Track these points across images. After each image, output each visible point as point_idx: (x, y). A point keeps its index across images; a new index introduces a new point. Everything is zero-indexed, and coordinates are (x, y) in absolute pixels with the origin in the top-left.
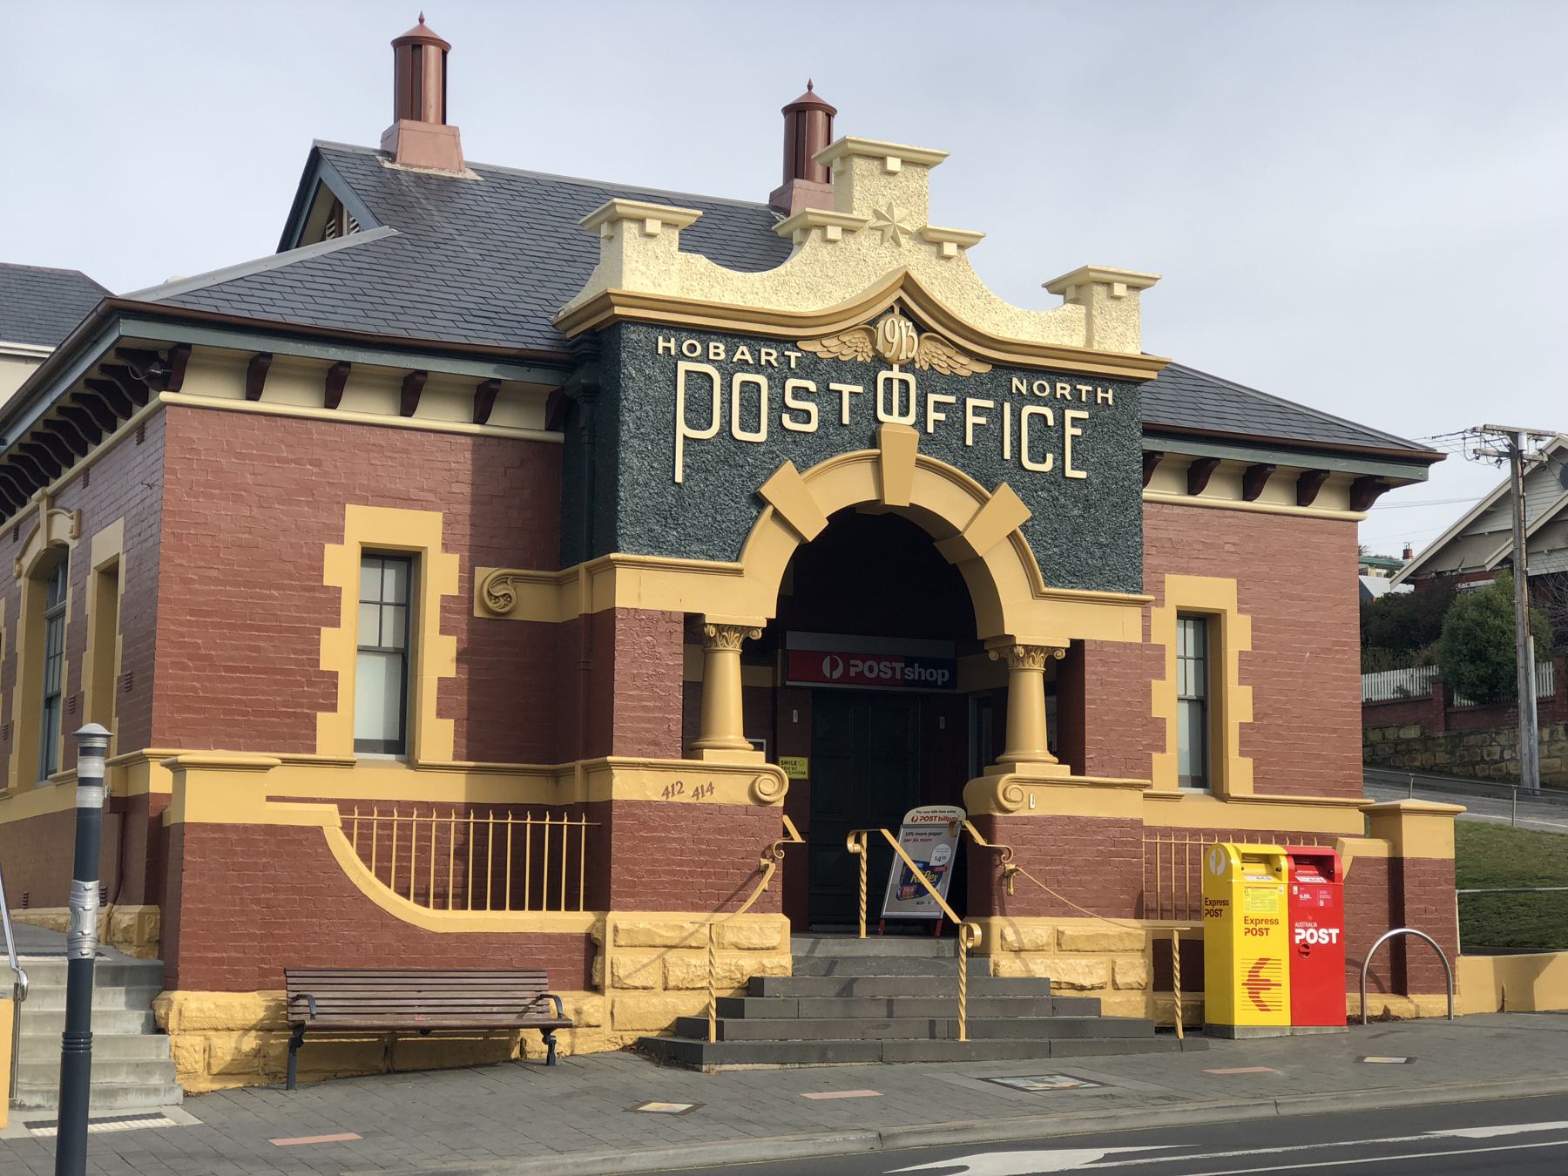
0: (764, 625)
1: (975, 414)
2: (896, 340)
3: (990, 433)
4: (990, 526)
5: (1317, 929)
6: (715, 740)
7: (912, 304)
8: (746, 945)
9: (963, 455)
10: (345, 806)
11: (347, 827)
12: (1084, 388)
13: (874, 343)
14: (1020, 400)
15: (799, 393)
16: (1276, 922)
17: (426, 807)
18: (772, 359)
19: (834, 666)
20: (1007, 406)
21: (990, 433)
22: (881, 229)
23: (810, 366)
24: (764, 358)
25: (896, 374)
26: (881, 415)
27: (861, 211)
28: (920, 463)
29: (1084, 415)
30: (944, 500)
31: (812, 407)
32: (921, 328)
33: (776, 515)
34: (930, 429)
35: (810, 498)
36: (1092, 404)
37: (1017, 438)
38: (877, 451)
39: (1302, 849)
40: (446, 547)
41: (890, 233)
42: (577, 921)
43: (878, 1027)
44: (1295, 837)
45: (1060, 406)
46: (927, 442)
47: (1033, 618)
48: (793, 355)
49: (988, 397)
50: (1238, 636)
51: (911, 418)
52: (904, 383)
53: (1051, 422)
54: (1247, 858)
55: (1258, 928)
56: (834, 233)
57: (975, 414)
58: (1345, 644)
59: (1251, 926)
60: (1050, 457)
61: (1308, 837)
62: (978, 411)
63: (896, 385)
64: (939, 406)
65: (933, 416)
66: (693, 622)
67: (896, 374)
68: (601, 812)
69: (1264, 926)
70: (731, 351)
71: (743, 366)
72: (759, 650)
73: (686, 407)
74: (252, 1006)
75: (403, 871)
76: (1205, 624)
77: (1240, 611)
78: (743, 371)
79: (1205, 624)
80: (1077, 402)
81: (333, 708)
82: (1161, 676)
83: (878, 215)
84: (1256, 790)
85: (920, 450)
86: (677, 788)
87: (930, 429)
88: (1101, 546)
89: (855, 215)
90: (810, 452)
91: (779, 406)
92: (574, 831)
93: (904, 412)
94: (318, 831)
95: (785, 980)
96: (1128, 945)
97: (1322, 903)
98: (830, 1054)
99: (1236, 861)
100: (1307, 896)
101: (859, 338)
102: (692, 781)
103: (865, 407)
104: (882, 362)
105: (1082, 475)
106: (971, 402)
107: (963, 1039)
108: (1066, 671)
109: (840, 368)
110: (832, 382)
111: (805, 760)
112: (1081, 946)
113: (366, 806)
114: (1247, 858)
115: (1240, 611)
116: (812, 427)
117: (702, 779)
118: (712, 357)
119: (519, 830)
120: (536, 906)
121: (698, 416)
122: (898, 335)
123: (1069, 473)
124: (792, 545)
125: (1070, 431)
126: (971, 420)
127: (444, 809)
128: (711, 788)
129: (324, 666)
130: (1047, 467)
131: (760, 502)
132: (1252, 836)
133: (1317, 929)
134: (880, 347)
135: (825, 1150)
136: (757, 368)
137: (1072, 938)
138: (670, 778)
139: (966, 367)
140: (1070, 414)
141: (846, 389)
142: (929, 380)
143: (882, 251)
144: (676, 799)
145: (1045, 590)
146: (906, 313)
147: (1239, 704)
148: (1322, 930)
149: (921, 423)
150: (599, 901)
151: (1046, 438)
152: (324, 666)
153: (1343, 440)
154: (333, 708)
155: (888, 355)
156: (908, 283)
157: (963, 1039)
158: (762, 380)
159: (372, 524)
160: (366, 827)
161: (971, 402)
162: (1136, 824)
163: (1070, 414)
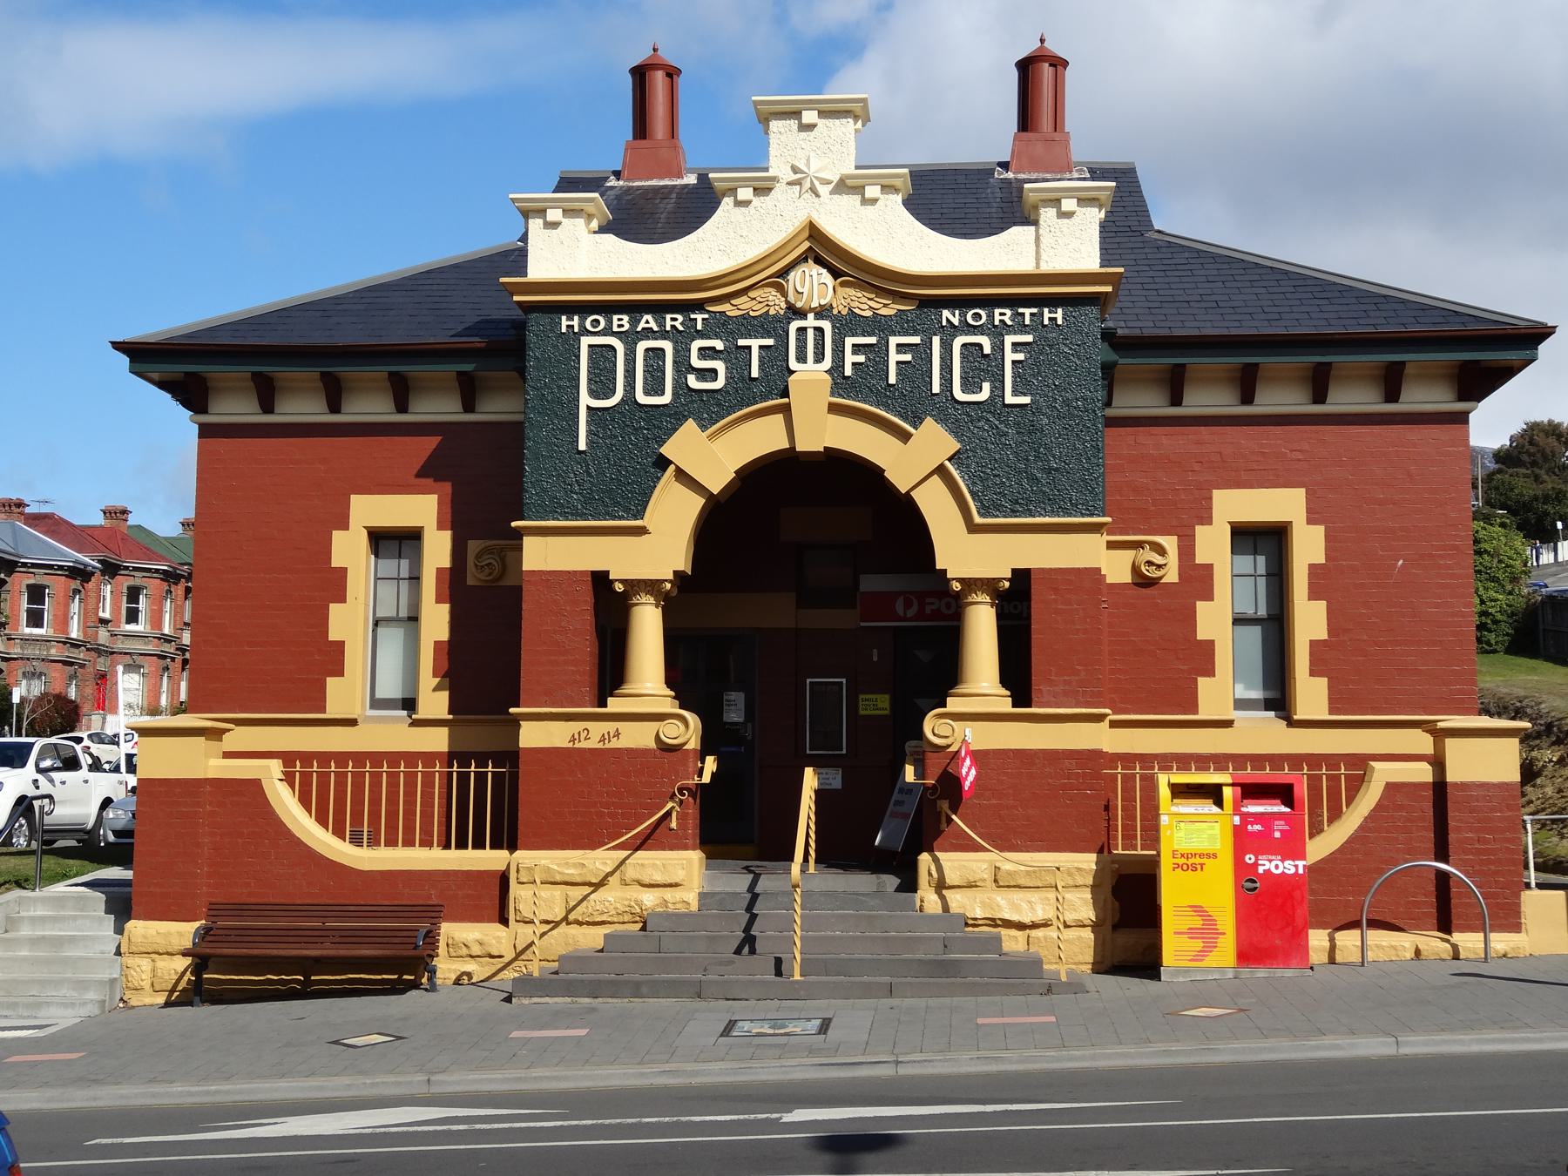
0: (671, 577)
1: (898, 352)
2: (806, 291)
3: (916, 370)
4: (913, 459)
5: (1282, 861)
6: (627, 689)
7: (819, 248)
8: (647, 881)
9: (885, 395)
10: (288, 758)
11: (288, 778)
12: (1027, 311)
13: (784, 294)
14: (953, 330)
15: (705, 353)
16: (1215, 856)
17: (411, 758)
18: (677, 324)
19: (908, 605)
20: (936, 340)
21: (916, 370)
22: (798, 183)
23: (719, 326)
24: (669, 324)
25: (811, 321)
26: (793, 364)
27: (778, 167)
28: (834, 409)
29: (1029, 338)
30: (757, 438)
31: (719, 366)
32: (836, 273)
33: (681, 475)
34: (848, 372)
35: (713, 456)
36: (1037, 325)
37: (946, 370)
38: (785, 400)
39: (1250, 774)
40: (440, 527)
41: (807, 185)
42: (490, 859)
43: (721, 964)
44: (1239, 760)
45: (997, 332)
46: (840, 383)
47: (964, 551)
48: (699, 317)
49: (915, 333)
50: (1308, 547)
51: (827, 363)
52: (819, 330)
53: (987, 350)
54: (1180, 791)
55: (1192, 863)
56: (745, 193)
57: (898, 352)
58: (1456, 548)
59: (1182, 861)
60: (986, 386)
61: (1258, 760)
62: (901, 348)
63: (810, 334)
64: (857, 349)
65: (850, 358)
66: (600, 580)
67: (811, 321)
68: (510, 756)
69: (1198, 860)
70: (634, 322)
71: (648, 333)
72: (679, 599)
73: (590, 380)
74: (183, 932)
75: (340, 812)
76: (1263, 541)
77: (1310, 521)
78: (648, 338)
79: (1263, 541)
80: (1022, 328)
81: (341, 673)
82: (1209, 596)
83: (795, 170)
84: (1331, 713)
85: (832, 395)
86: (583, 735)
87: (848, 372)
88: (1049, 471)
89: (771, 173)
90: (709, 410)
91: (682, 366)
92: (481, 778)
93: (819, 357)
94: (256, 783)
95: (689, 915)
96: (1080, 881)
97: (1277, 835)
98: (644, 990)
99: (1164, 792)
100: (1258, 827)
101: (772, 295)
102: (598, 729)
103: (776, 360)
104: (796, 312)
105: (1026, 400)
106: (894, 341)
107: (797, 977)
108: (1016, 597)
109: (752, 326)
110: (736, 336)
111: (887, 697)
112: (1022, 882)
113: (306, 757)
114: (1180, 791)
115: (1310, 521)
116: (719, 383)
117: (610, 726)
118: (615, 329)
119: (393, 777)
120: (409, 843)
121: (601, 386)
122: (813, 285)
123: (1010, 399)
124: (699, 502)
125: (1010, 356)
126: (894, 357)
127: (429, 758)
128: (617, 734)
129: (333, 636)
130: (984, 394)
131: (663, 463)
132: (1183, 761)
133: (1282, 861)
134: (791, 298)
135: (1102, 1064)
136: (663, 335)
137: (1009, 873)
138: (576, 727)
139: (889, 309)
140: (1009, 340)
141: (755, 344)
142: (847, 324)
143: (801, 203)
144: (584, 745)
145: (978, 520)
146: (819, 261)
147: (1310, 621)
148: (1287, 863)
149: (837, 368)
150: (507, 839)
151: (981, 366)
152: (333, 636)
153: (1454, 327)
154: (341, 673)
155: (799, 305)
156: (814, 232)
157: (797, 977)
158: (667, 346)
159: (372, 510)
160: (306, 777)
161: (894, 341)
162: (1097, 754)
163: (1009, 340)
